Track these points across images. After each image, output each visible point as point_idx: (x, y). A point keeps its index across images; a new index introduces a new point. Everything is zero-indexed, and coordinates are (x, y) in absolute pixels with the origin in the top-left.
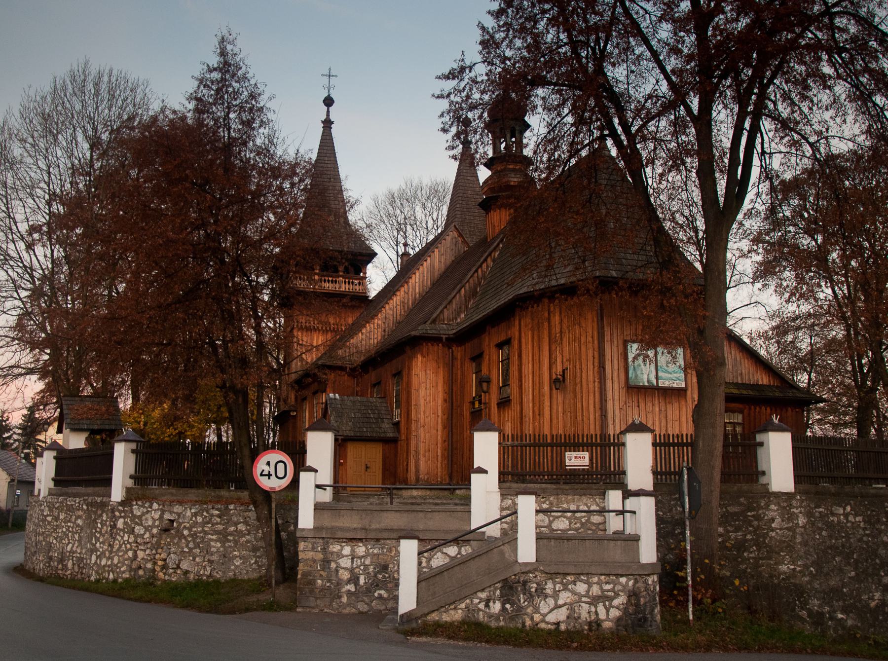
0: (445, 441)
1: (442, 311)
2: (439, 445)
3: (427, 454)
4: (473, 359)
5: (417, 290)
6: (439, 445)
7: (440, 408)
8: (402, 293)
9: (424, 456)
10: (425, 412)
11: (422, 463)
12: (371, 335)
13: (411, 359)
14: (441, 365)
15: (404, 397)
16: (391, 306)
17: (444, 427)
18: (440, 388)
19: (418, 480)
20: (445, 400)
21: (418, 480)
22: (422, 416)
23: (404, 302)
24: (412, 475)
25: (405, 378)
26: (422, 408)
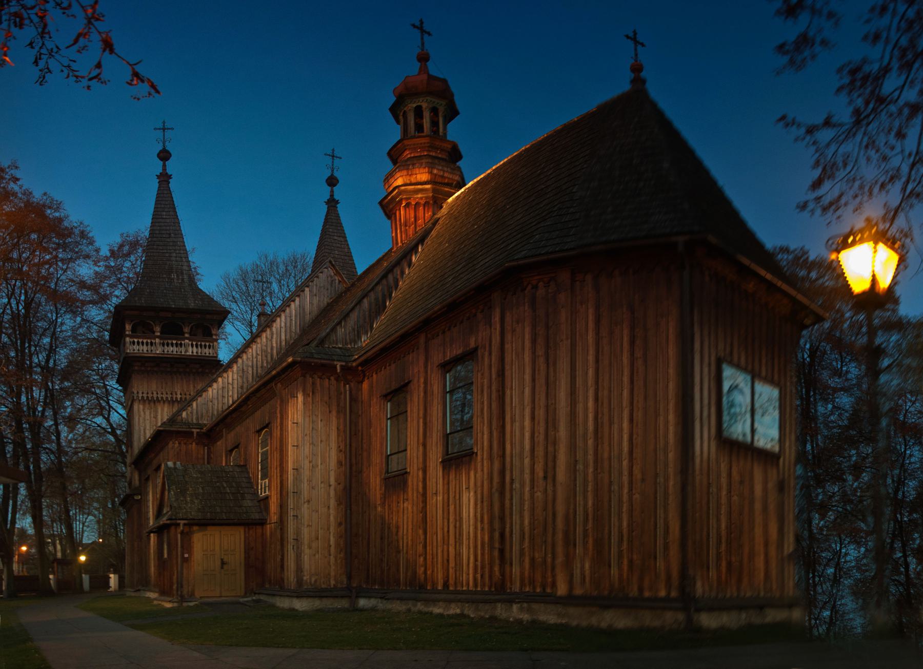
0: (340, 524)
1: (333, 329)
2: (332, 529)
3: (314, 545)
4: (389, 396)
5: (283, 337)
6: (332, 529)
7: (332, 474)
8: (264, 340)
9: (310, 548)
10: (310, 481)
11: (306, 558)
12: (223, 392)
13: (284, 403)
14: (334, 413)
15: (274, 463)
17: (339, 503)
18: (334, 445)
19: (300, 582)
20: (340, 463)
21: (300, 582)
22: (305, 486)
23: (266, 351)
24: (290, 576)
25: (277, 433)
26: (306, 474)
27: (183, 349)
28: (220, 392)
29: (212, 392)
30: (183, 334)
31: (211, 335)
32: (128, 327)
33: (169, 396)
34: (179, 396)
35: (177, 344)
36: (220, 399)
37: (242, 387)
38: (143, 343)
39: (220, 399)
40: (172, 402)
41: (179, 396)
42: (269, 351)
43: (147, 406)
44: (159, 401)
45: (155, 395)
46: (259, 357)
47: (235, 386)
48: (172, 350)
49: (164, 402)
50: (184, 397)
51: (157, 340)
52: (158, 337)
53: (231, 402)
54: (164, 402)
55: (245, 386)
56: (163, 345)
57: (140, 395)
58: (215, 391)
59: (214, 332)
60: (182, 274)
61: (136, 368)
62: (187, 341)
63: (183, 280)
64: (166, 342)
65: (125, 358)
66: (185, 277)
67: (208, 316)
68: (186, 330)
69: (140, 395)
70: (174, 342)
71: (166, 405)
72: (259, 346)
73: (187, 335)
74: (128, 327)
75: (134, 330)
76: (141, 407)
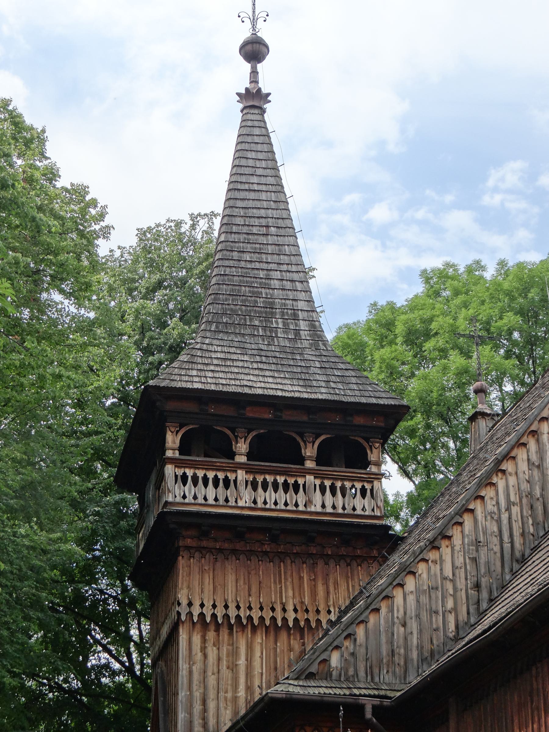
8: (523, 466)
16: (490, 506)
23: (530, 495)
27: (301, 498)
28: (424, 599)
29: (405, 600)
30: (301, 460)
31: (365, 464)
32: (172, 440)
33: (268, 615)
34: (291, 616)
35: (286, 485)
36: (425, 616)
37: (477, 586)
38: (205, 480)
39: (425, 616)
40: (274, 629)
41: (291, 616)
42: (537, 492)
43: (211, 635)
44: (243, 627)
45: (232, 612)
46: (515, 510)
47: (461, 584)
48: (274, 501)
49: (254, 629)
50: (302, 617)
51: (241, 475)
52: (241, 466)
53: (452, 626)
54: (254, 629)
55: (484, 581)
56: (255, 489)
57: (196, 611)
58: (411, 599)
59: (372, 457)
60: (295, 317)
61: (189, 542)
62: (310, 478)
63: (297, 332)
64: (260, 479)
65: (162, 515)
66: (303, 325)
67: (359, 420)
68: (310, 451)
69: (196, 611)
70: (281, 479)
71: (259, 639)
72: (512, 480)
73: (310, 464)
74: (172, 440)
75: (184, 449)
76: (197, 639)
